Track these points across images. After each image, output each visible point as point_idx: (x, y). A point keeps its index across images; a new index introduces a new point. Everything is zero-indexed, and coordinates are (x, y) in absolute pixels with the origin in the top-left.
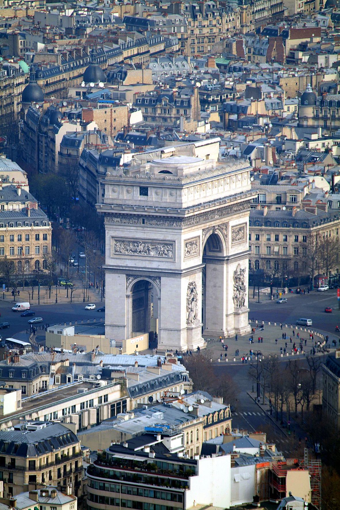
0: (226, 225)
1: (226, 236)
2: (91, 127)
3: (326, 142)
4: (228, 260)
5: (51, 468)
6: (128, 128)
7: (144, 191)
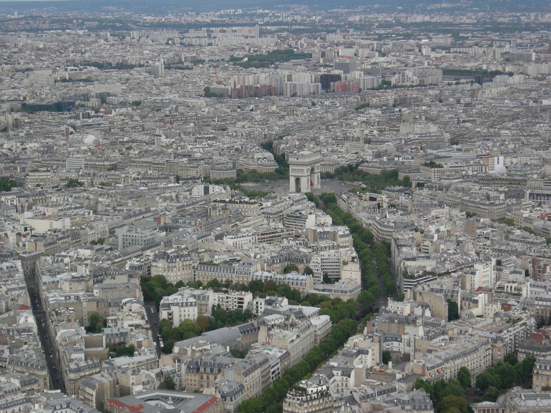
2: (288, 145)
4: (316, 173)
7: (297, 159)
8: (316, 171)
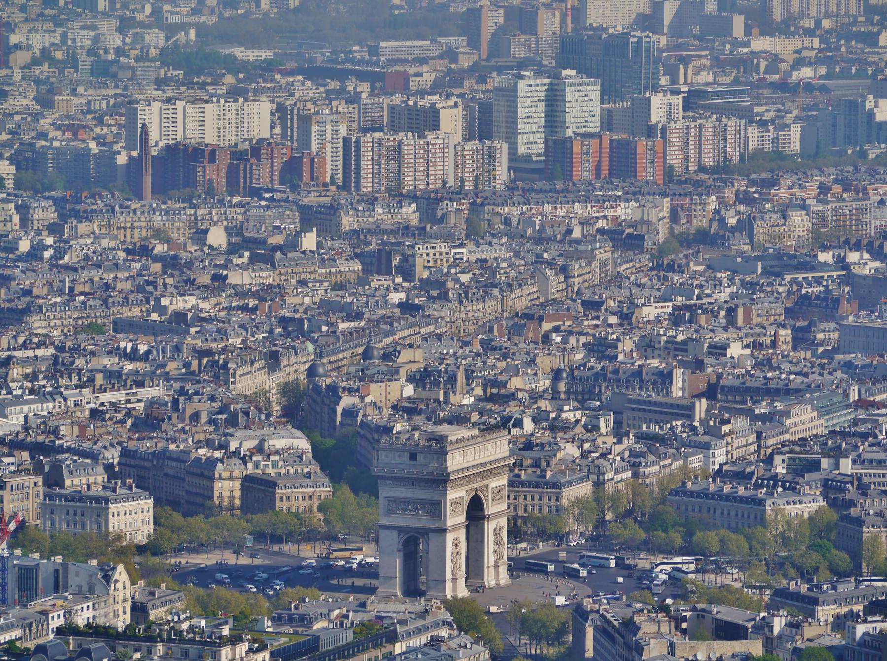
0: (487, 486)
2: (368, 400)
3: (577, 413)
6: (400, 401)
8: (491, 508)
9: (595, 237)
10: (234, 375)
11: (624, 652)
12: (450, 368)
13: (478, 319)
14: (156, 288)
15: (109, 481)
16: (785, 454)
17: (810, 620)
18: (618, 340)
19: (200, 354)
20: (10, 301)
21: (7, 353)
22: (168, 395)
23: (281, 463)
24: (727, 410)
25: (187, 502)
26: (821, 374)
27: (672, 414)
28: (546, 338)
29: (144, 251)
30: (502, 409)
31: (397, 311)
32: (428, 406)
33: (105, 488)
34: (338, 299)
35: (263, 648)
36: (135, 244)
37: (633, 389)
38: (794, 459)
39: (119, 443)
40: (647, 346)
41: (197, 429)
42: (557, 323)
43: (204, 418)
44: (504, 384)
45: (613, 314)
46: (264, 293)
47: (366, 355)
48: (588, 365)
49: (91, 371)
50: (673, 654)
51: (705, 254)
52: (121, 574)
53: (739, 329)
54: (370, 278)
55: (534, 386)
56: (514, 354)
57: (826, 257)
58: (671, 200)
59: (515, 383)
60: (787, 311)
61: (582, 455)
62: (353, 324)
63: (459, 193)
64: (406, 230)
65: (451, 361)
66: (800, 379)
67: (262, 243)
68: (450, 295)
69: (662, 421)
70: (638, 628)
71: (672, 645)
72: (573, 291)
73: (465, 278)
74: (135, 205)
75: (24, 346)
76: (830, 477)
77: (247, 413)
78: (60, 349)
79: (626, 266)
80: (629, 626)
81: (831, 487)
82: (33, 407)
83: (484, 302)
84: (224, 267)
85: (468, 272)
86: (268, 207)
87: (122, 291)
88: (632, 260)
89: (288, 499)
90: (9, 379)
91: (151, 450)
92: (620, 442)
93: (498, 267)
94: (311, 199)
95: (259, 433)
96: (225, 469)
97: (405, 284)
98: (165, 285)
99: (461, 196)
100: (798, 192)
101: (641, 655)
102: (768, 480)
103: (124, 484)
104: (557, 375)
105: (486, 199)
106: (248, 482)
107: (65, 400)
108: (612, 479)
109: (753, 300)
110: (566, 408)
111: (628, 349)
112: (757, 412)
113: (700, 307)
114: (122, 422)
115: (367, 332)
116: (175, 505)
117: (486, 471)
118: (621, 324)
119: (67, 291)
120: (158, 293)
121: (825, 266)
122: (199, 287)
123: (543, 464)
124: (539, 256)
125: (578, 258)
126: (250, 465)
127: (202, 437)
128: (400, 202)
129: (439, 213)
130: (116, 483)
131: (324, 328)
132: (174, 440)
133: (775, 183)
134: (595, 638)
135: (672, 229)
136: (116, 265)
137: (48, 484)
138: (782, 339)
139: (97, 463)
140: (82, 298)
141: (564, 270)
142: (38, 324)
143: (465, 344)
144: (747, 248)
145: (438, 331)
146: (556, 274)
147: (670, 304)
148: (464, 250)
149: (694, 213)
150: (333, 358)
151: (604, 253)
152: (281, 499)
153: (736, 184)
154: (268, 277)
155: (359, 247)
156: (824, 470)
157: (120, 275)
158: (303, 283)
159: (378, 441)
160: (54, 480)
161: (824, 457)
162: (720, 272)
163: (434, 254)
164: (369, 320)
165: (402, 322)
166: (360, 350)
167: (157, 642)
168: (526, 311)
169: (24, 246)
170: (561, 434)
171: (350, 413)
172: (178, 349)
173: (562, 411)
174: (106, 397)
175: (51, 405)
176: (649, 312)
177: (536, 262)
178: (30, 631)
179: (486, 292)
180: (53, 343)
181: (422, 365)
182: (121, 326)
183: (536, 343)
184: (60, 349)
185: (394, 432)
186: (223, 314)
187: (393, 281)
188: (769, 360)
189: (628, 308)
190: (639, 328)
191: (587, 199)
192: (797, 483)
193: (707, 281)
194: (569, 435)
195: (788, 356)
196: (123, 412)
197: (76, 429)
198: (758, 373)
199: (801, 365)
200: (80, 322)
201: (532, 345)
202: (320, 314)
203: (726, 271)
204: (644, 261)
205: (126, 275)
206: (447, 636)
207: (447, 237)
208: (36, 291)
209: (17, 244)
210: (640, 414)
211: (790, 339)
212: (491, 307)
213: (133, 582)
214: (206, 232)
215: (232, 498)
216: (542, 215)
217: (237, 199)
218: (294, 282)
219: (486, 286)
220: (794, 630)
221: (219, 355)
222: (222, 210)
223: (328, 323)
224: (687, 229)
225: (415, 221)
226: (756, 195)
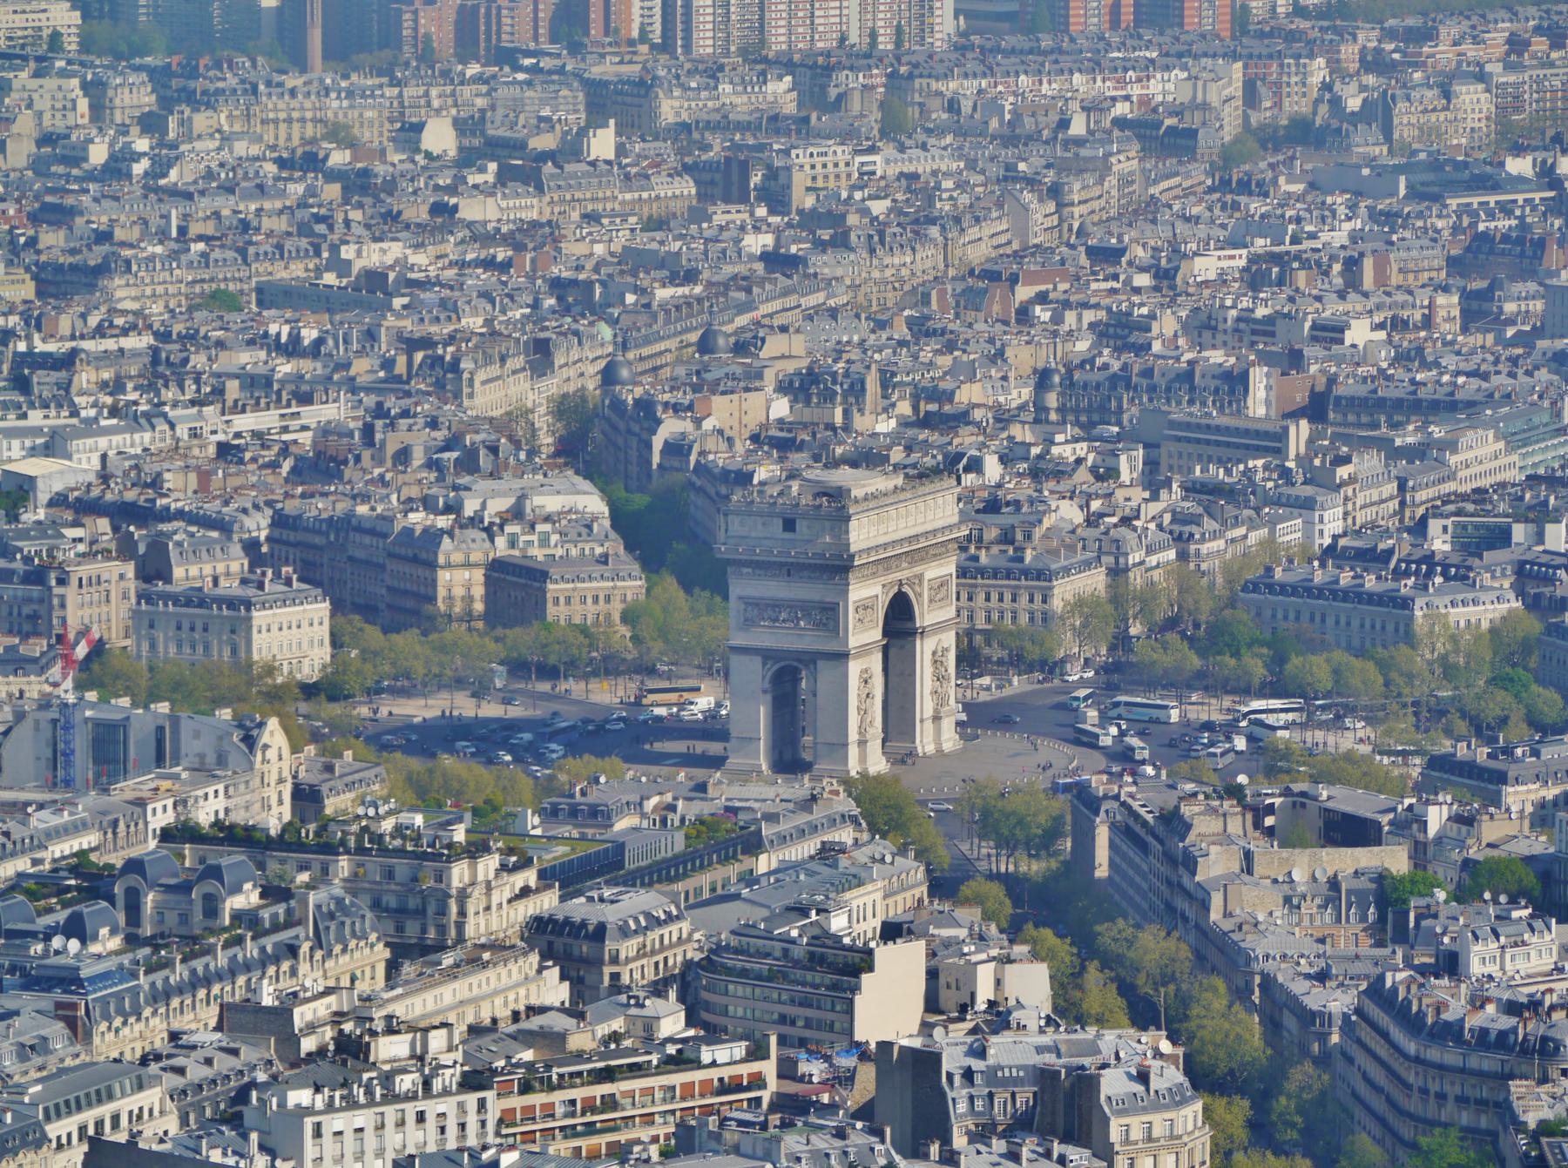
0: (920, 577)
1: (920, 595)
2: (708, 425)
3: (1078, 446)
5: (644, 961)
6: (765, 426)
8: (925, 616)
9: (1109, 132)
10: (471, 381)
11: (1164, 869)
12: (853, 368)
13: (902, 281)
14: (331, 228)
15: (251, 571)
16: (1447, 517)
17: (1492, 810)
18: (1152, 316)
19: (411, 344)
20: (73, 252)
21: (69, 345)
22: (353, 418)
23: (554, 538)
24: (1346, 439)
25: (389, 606)
26: (1512, 375)
27: (1247, 447)
28: (1024, 314)
29: (311, 162)
30: (946, 439)
31: (759, 267)
32: (814, 435)
33: (244, 582)
34: (654, 246)
35: (525, 863)
36: (293, 151)
37: (1179, 403)
38: (1464, 527)
39: (269, 504)
40: (1203, 327)
41: (407, 478)
42: (1043, 288)
43: (418, 458)
44: (949, 396)
45: (1142, 270)
46: (521, 236)
47: (705, 345)
48: (1099, 362)
49: (219, 375)
50: (1250, 872)
51: (1307, 161)
52: (273, 734)
53: (1366, 295)
54: (711, 209)
55: (1001, 399)
56: (967, 342)
57: (1519, 166)
58: (1246, 66)
59: (968, 394)
60: (1452, 262)
61: (1087, 520)
62: (680, 291)
63: (868, 56)
64: (775, 122)
65: (855, 355)
66: (1475, 383)
67: (519, 146)
68: (853, 237)
69: (1229, 460)
70: (1189, 827)
71: (1248, 856)
72: (1070, 229)
73: (879, 208)
74: (293, 81)
75: (100, 332)
76: (1528, 557)
77: (494, 450)
78: (164, 336)
79: (1165, 185)
80: (1173, 822)
81: (1530, 575)
82: (117, 439)
83: (913, 249)
84: (452, 190)
85: (885, 197)
86: (529, 83)
87: (270, 234)
88: (1176, 174)
89: (568, 601)
90: (74, 390)
91: (324, 516)
92: (1155, 497)
93: (938, 187)
94: (605, 69)
95: (517, 484)
96: (457, 549)
97: (775, 220)
98: (347, 223)
99: (872, 62)
100: (1471, 51)
101: (1194, 873)
102: (1419, 562)
103: (277, 575)
104: (1042, 378)
105: (916, 66)
106: (497, 570)
107: (172, 426)
108: (1142, 563)
109: (1392, 243)
110: (1059, 438)
111: (1169, 333)
112: (1398, 442)
113: (1297, 257)
114: (274, 465)
115: (707, 304)
116: (368, 611)
117: (918, 551)
118: (1156, 289)
119: (174, 234)
120: (335, 237)
121: (1519, 182)
122: (408, 227)
123: (1019, 536)
124: (1011, 167)
125: (1081, 171)
126: (501, 542)
127: (414, 492)
128: (763, 73)
129: (833, 93)
130: (264, 574)
131: (630, 298)
132: (365, 498)
133: (1429, 35)
134: (1112, 845)
135: (1246, 118)
136: (260, 187)
137: (144, 575)
138: (1442, 313)
139: (230, 538)
140: (201, 246)
141: (1055, 192)
142: (123, 293)
143: (881, 325)
144: (1381, 150)
145: (832, 303)
146: (1041, 200)
147: (1244, 252)
148: (877, 158)
149: (1286, 90)
150: (646, 351)
151: (1126, 162)
152: (556, 601)
153: (1361, 36)
154: (529, 207)
155: (690, 154)
156: (1518, 544)
157: (267, 205)
158: (591, 218)
159: (727, 498)
160: (153, 568)
161: (1518, 521)
162: (1332, 194)
163: (825, 166)
164: (710, 284)
165: (768, 287)
166: (694, 337)
167: (338, 854)
168: (987, 266)
169: (98, 154)
170: (1051, 484)
171: (676, 449)
172: (371, 336)
173: (1052, 443)
174: (246, 422)
175: (147, 436)
176: (1206, 266)
177: (1006, 179)
178: (115, 833)
179: (917, 233)
180: (150, 327)
181: (805, 363)
182: (269, 296)
183: (1006, 323)
184: (164, 336)
185: (755, 481)
186: (451, 273)
187: (752, 214)
188: (1420, 350)
189: (1169, 260)
190: (1188, 295)
191: (1095, 67)
192: (1470, 568)
193: (1309, 210)
194: (1065, 485)
195: (1453, 342)
196: (276, 449)
197: (193, 478)
198: (1399, 373)
199: (1477, 359)
200: (197, 289)
201: (999, 327)
202: (622, 272)
203: (1344, 191)
204: (1198, 174)
205: (278, 205)
206: (850, 842)
207: (846, 135)
208: (119, 234)
209: (85, 149)
210: (1191, 448)
211: (1456, 312)
212: (926, 259)
213: (295, 749)
214: (419, 128)
215: (469, 599)
216: (1015, 94)
217: (473, 69)
218: (575, 216)
219: (916, 222)
220: (1464, 829)
221: (445, 345)
222: (449, 89)
223: (636, 290)
224: (1274, 118)
225: (790, 107)
226: (1396, 56)
